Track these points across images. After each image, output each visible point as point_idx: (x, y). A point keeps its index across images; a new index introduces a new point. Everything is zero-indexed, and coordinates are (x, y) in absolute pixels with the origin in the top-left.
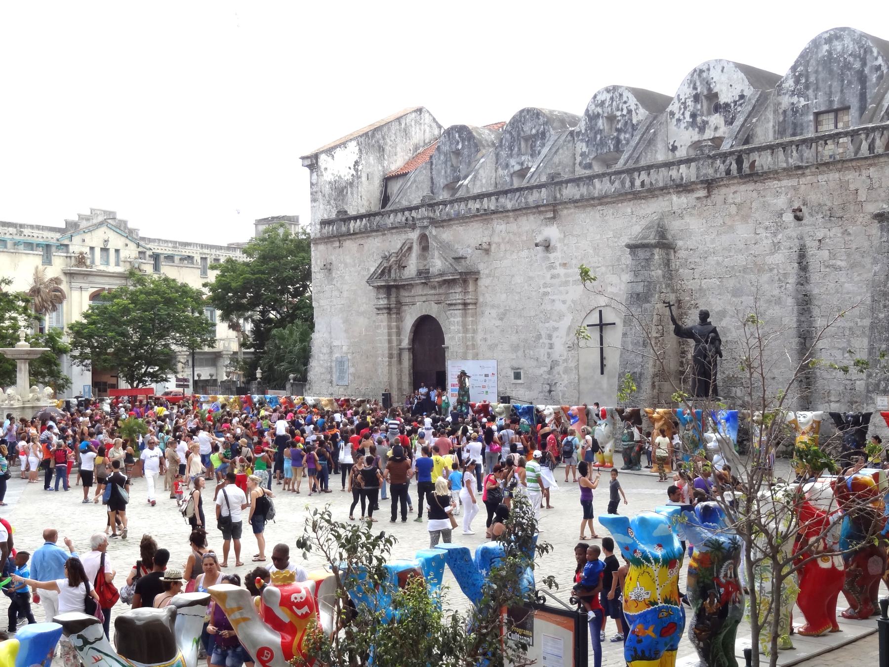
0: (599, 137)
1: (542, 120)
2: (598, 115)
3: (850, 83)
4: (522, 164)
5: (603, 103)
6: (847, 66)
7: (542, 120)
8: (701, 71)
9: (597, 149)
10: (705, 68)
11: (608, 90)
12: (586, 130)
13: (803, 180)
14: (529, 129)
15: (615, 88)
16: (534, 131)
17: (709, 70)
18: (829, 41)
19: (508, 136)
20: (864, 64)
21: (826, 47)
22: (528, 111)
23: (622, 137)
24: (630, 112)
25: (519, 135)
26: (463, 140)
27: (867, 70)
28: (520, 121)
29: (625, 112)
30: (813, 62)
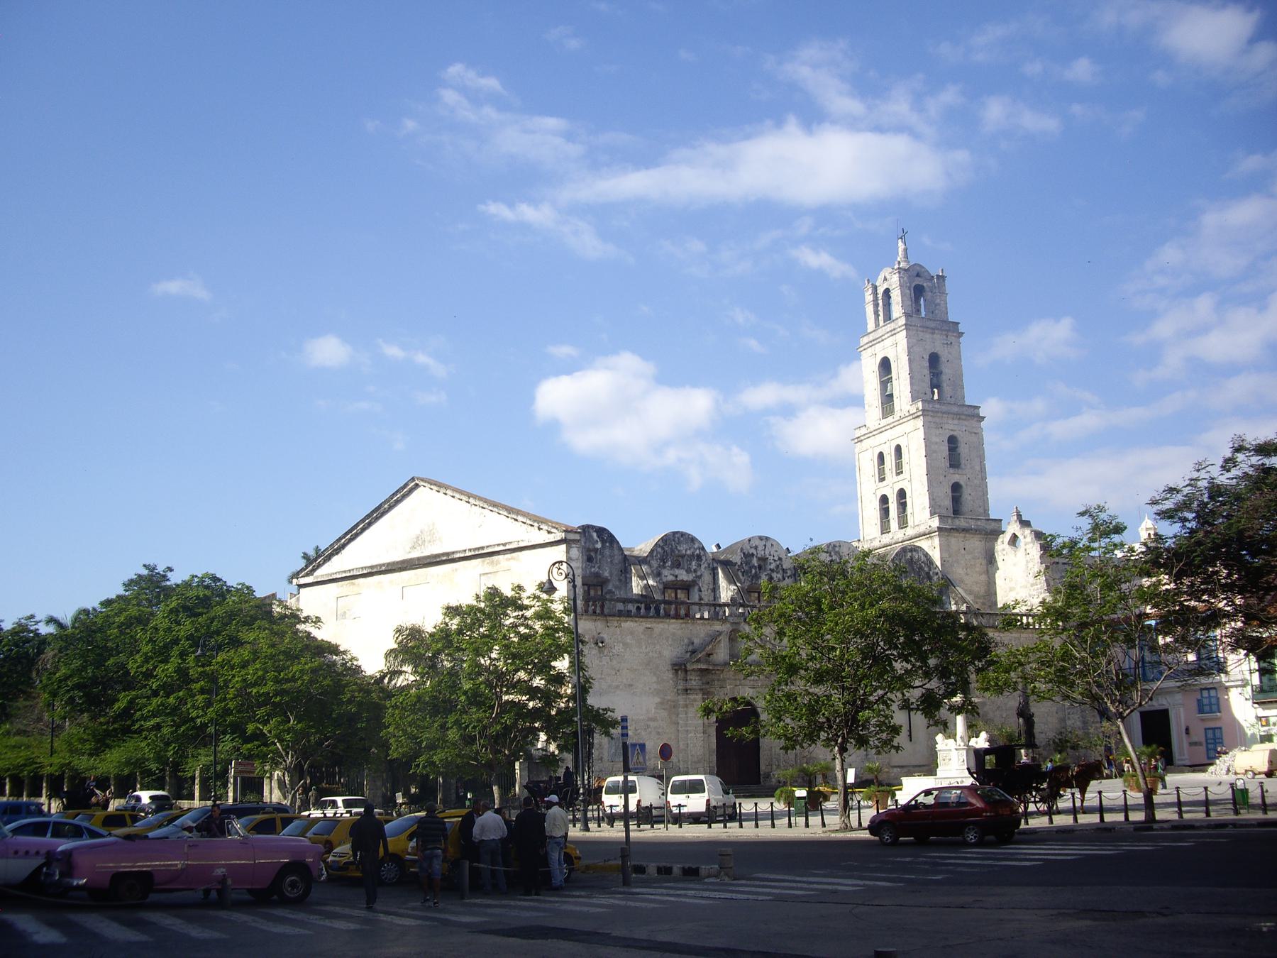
0: (753, 571)
1: (696, 546)
2: (753, 554)
3: (923, 578)
4: (676, 576)
5: (756, 548)
6: (921, 568)
7: (696, 546)
8: (835, 546)
9: (752, 580)
10: (838, 545)
11: (761, 538)
12: (741, 563)
13: (1022, 635)
14: (683, 548)
15: (767, 538)
16: (689, 552)
17: (840, 546)
18: (911, 551)
19: (659, 549)
20: (930, 570)
21: (909, 554)
22: (683, 534)
23: (774, 575)
24: (780, 559)
25: (672, 550)
26: (603, 542)
27: (931, 573)
28: (674, 540)
29: (776, 558)
30: (903, 560)
